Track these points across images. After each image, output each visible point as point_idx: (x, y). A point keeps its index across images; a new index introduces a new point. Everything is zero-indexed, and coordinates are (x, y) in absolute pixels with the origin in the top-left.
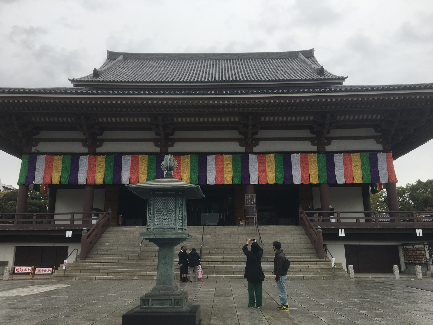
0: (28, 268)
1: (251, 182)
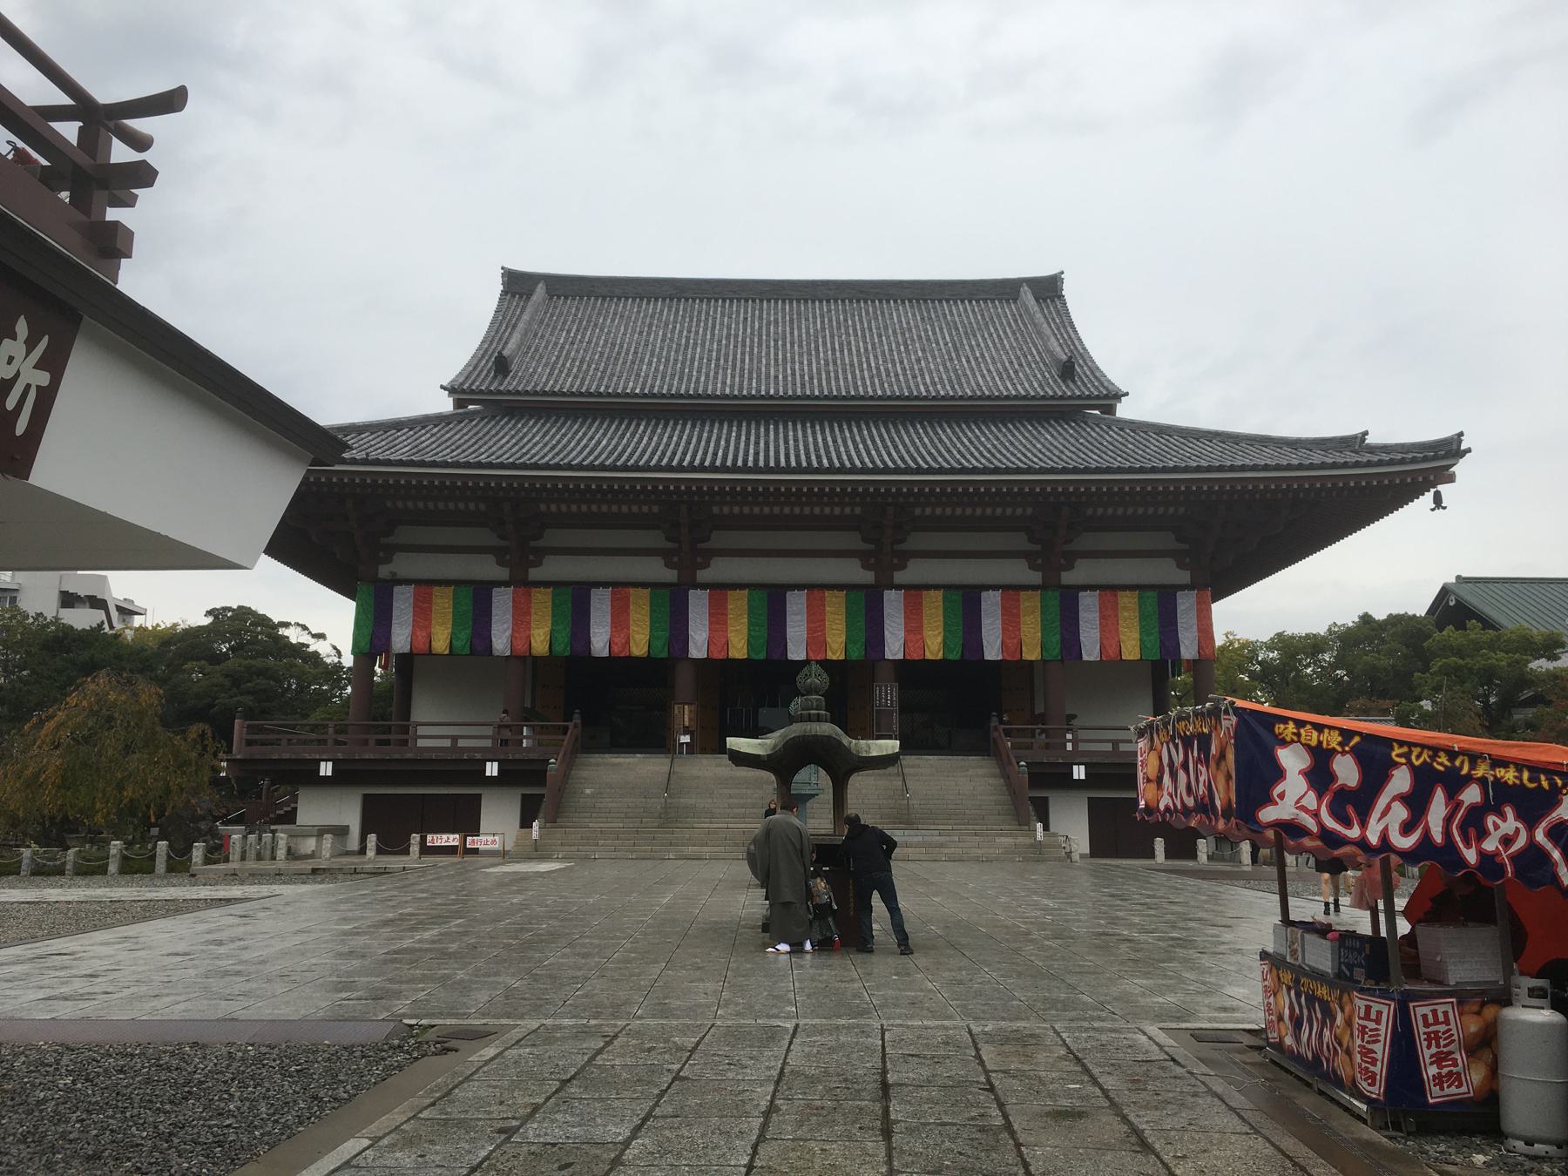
0: (452, 836)
1: (889, 656)
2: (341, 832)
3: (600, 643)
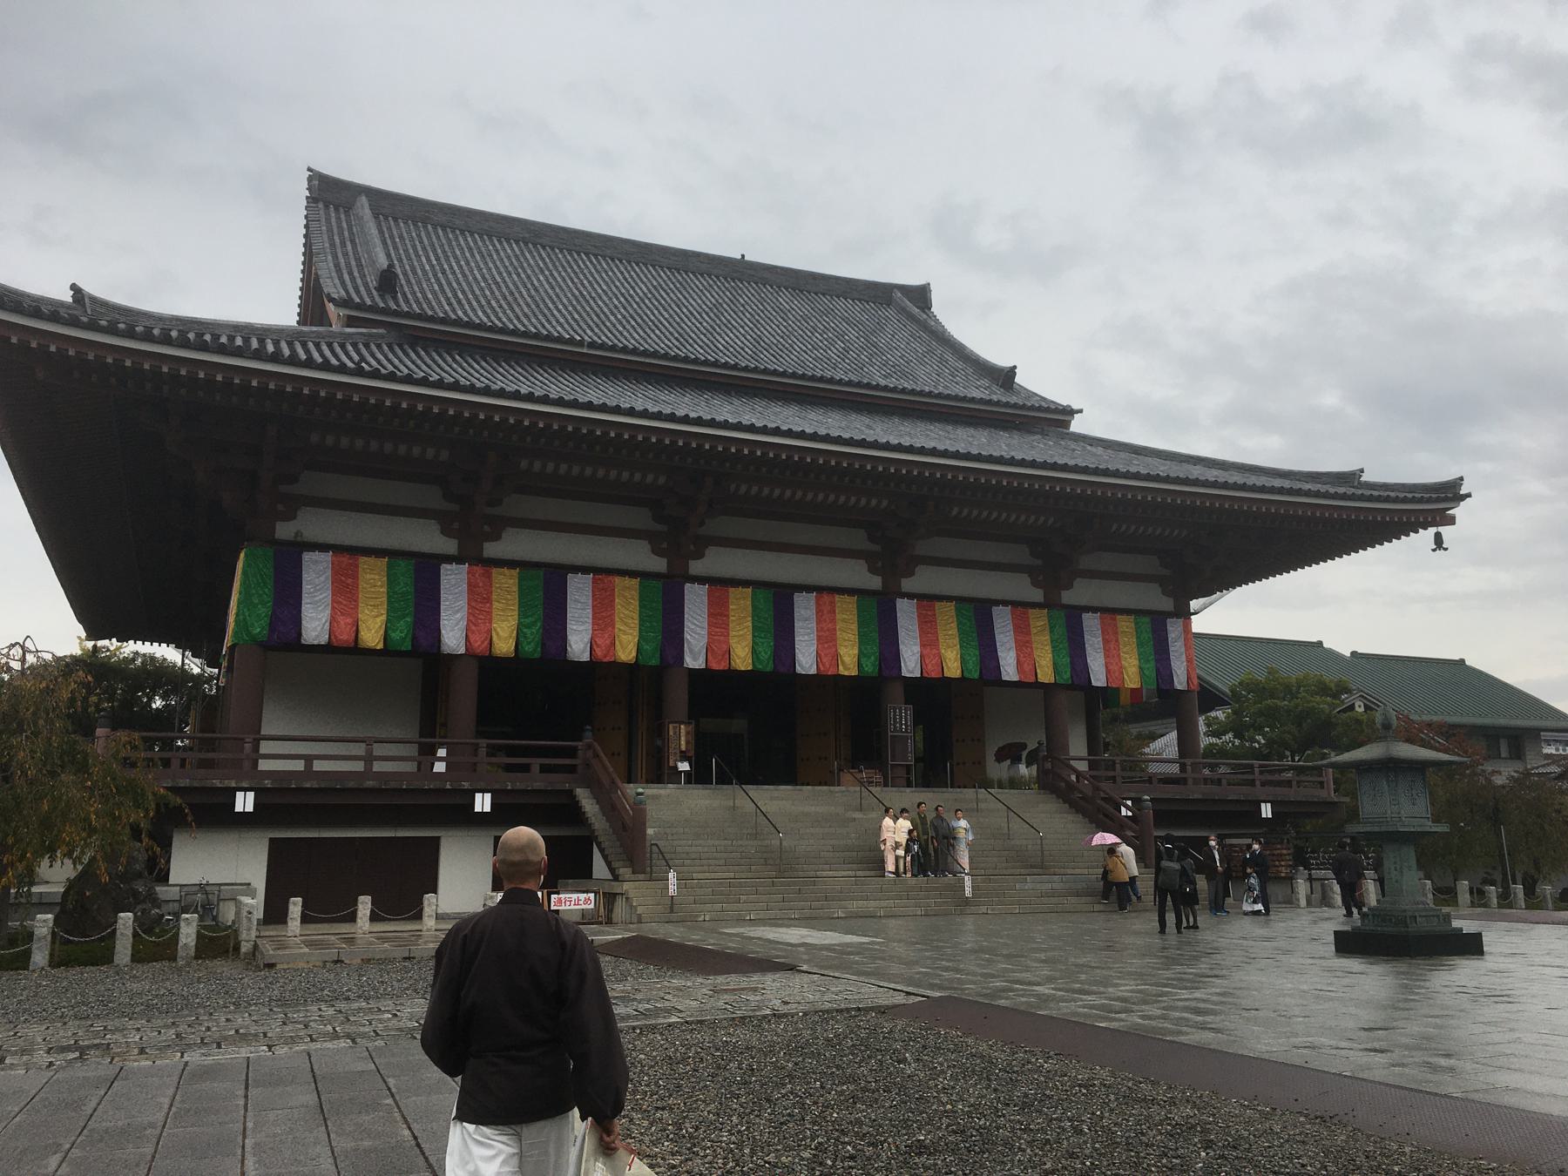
1: (905, 673)
3: (579, 644)
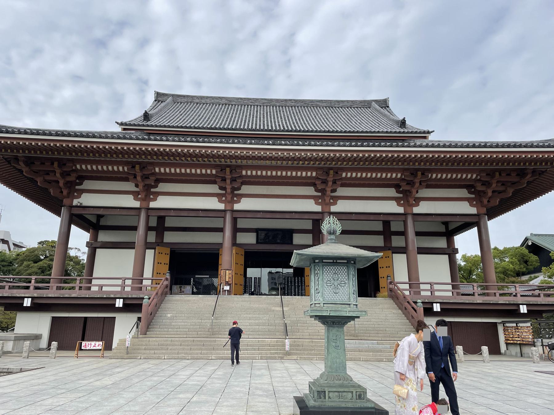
2: (38, 337)
